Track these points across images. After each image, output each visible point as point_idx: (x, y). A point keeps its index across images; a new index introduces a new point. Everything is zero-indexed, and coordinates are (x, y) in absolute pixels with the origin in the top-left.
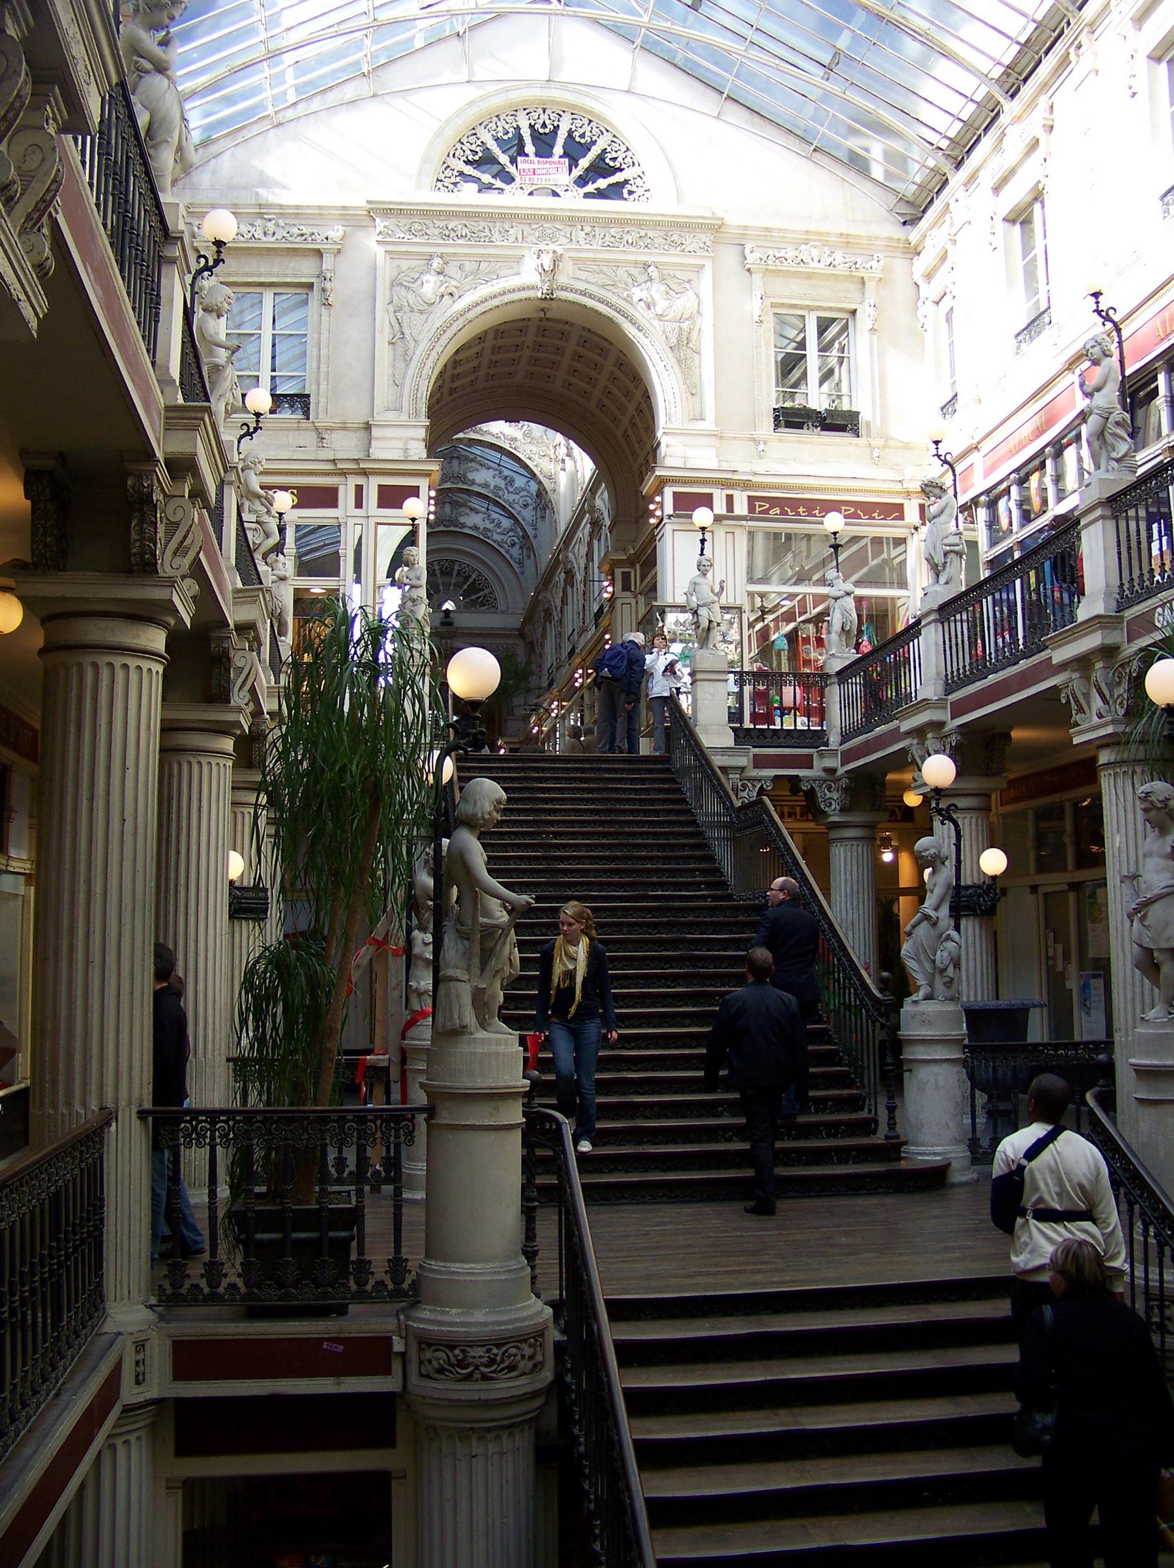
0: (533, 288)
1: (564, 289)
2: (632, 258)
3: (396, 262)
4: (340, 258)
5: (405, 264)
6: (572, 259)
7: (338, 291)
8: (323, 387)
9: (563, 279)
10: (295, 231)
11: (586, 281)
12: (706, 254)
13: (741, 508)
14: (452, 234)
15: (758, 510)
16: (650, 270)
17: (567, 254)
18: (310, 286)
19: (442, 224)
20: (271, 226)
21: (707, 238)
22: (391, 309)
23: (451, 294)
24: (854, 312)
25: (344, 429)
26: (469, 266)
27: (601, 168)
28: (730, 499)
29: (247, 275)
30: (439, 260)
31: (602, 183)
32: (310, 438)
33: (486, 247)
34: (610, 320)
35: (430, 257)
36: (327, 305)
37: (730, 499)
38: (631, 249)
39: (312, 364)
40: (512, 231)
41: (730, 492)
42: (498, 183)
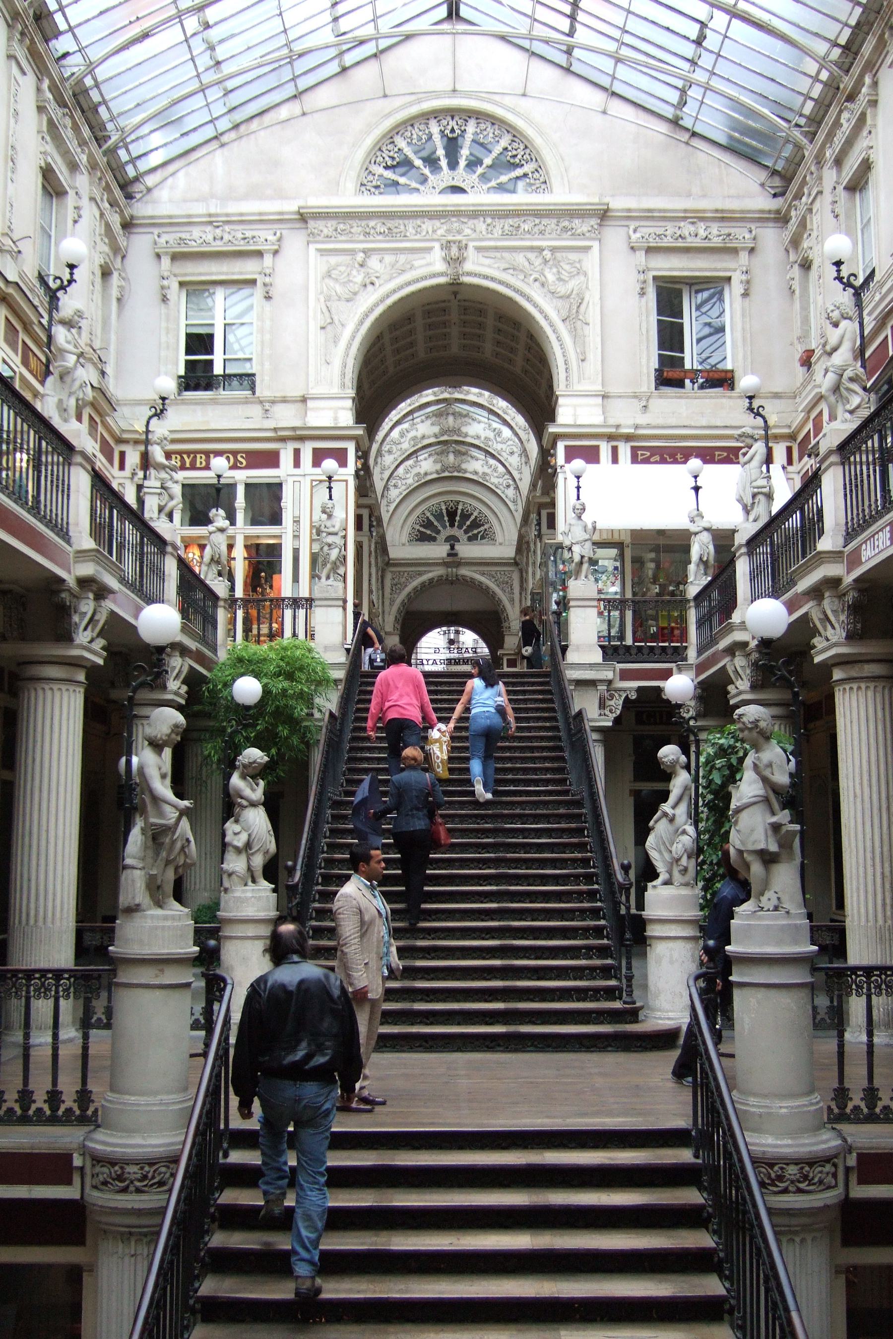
0: (441, 274)
1: (469, 274)
3: (325, 258)
4: (280, 259)
5: (333, 260)
7: (280, 284)
9: (468, 266)
10: (240, 236)
11: (489, 266)
12: (593, 235)
14: (372, 231)
15: (640, 458)
16: (545, 253)
17: (471, 245)
19: (364, 223)
20: (218, 232)
21: (594, 222)
22: (322, 300)
23: (372, 284)
24: (729, 279)
29: (200, 274)
30: (362, 255)
33: (401, 241)
34: (510, 299)
35: (352, 252)
38: (528, 236)
40: (424, 226)
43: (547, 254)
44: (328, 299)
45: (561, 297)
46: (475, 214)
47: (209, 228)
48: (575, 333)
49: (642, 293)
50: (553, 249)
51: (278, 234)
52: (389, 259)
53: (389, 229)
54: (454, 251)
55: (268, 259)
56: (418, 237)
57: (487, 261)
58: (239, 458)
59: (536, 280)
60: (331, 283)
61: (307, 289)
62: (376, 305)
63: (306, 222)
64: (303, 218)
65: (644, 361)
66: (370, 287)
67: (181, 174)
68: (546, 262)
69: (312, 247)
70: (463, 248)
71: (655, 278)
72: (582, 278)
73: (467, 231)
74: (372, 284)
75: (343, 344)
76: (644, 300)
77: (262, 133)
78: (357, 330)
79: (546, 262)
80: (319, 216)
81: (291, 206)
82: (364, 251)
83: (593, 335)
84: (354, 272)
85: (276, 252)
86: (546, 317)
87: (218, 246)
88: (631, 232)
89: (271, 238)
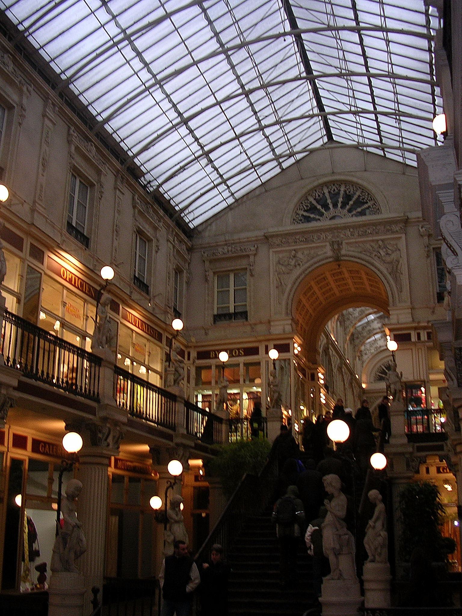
1: (344, 256)
2: (371, 239)
5: (281, 255)
6: (347, 243)
8: (252, 306)
13: (424, 337)
17: (344, 242)
18: (246, 269)
22: (276, 274)
23: (299, 265)
25: (261, 323)
26: (306, 252)
27: (359, 203)
28: (419, 335)
30: (294, 252)
31: (359, 210)
32: (248, 328)
35: (290, 251)
36: (252, 275)
37: (419, 335)
39: (248, 299)
41: (419, 331)
42: (317, 217)
43: (380, 243)
44: (279, 273)
45: (388, 263)
46: (345, 227)
47: (226, 247)
48: (396, 280)
49: (428, 256)
50: (383, 240)
51: (256, 246)
52: (306, 252)
53: (306, 239)
54: (336, 247)
55: (252, 259)
56: (319, 241)
57: (352, 249)
58: (241, 351)
59: (375, 255)
60: (280, 266)
61: (269, 270)
62: (301, 274)
63: (268, 239)
64: (266, 238)
65: (431, 289)
66: (298, 267)
67: (213, 224)
68: (380, 247)
69: (271, 251)
70: (339, 244)
71: (433, 249)
72: (398, 252)
73: (342, 236)
74: (299, 265)
75: (286, 295)
76: (429, 261)
77: (248, 202)
78: (292, 287)
79: (380, 247)
80: (272, 236)
81: (260, 233)
82: (295, 250)
83: (405, 279)
84: (291, 260)
85: (255, 255)
86: (381, 273)
87: (230, 255)
88: (420, 228)
89: (253, 248)
